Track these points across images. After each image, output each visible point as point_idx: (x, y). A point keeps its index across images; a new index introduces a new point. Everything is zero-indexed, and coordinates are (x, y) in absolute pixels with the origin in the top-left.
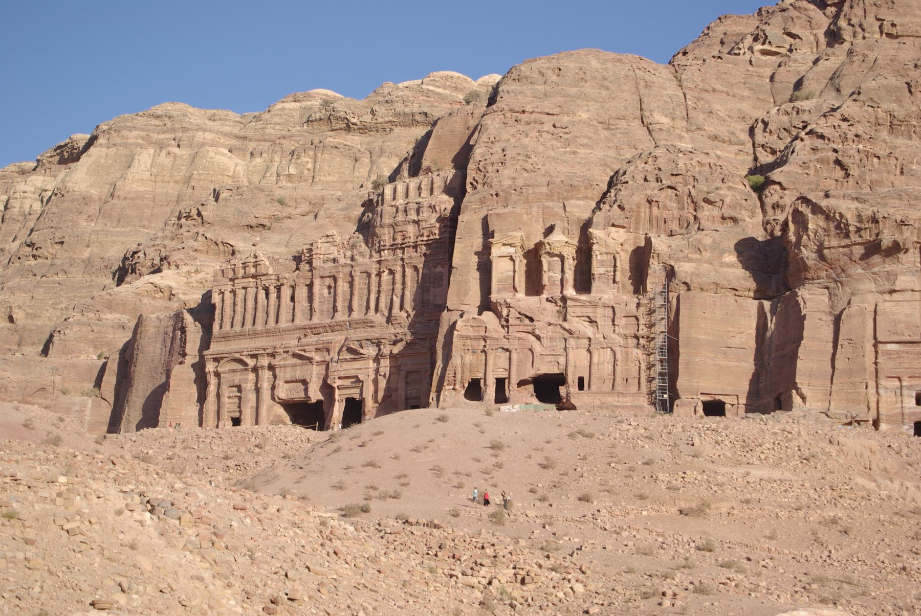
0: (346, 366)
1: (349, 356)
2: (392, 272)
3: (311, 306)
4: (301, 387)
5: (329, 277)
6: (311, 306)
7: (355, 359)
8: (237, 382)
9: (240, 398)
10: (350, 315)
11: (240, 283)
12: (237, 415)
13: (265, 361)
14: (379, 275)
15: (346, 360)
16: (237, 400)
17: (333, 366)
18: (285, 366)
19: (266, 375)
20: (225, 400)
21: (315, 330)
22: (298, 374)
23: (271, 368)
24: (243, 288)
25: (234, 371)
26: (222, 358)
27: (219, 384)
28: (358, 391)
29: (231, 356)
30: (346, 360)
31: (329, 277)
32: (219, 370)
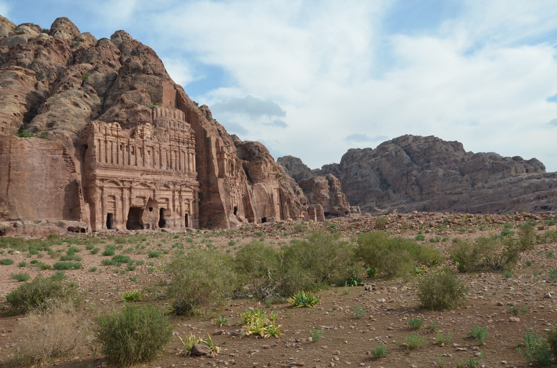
0: (162, 193)
1: (164, 188)
2: (175, 151)
3: (144, 159)
4: (142, 200)
5: (150, 147)
6: (144, 159)
7: (167, 190)
8: (113, 194)
9: (114, 203)
10: (160, 168)
11: (109, 138)
12: (112, 212)
13: (127, 185)
14: (171, 151)
15: (163, 190)
16: (112, 204)
17: (157, 193)
18: (137, 189)
19: (126, 192)
20: (106, 203)
21: (148, 172)
22: (142, 194)
23: (130, 189)
24: (111, 141)
25: (112, 188)
26: (106, 180)
27: (102, 194)
28: (166, 205)
29: (112, 179)
30: (163, 190)
31: (150, 147)
32: (105, 186)
